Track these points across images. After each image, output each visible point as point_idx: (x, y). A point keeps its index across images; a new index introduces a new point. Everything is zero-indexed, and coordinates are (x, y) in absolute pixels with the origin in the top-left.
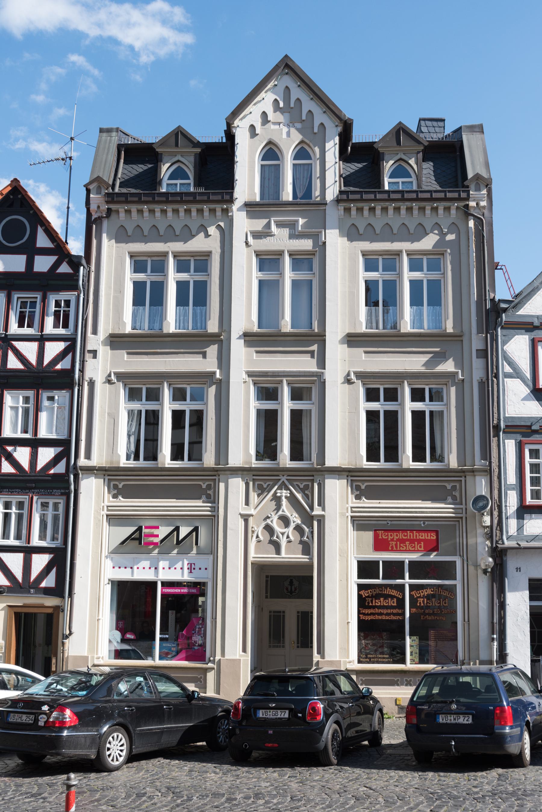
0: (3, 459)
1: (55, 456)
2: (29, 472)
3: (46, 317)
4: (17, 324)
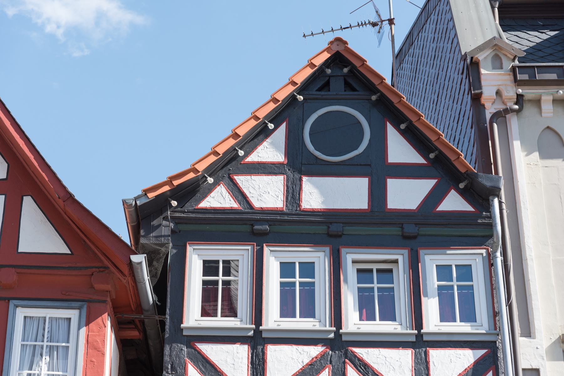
3: (423, 299)
4: (357, 314)
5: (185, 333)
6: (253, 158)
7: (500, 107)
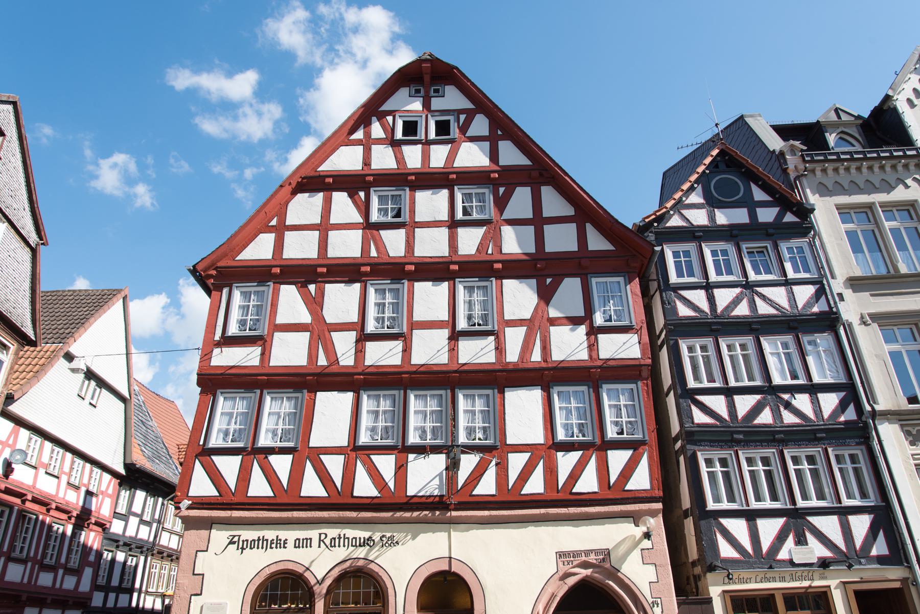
0: (782, 409)
1: (840, 402)
2: (816, 421)
5: (671, 286)
6: (688, 201)
7: (797, 174)
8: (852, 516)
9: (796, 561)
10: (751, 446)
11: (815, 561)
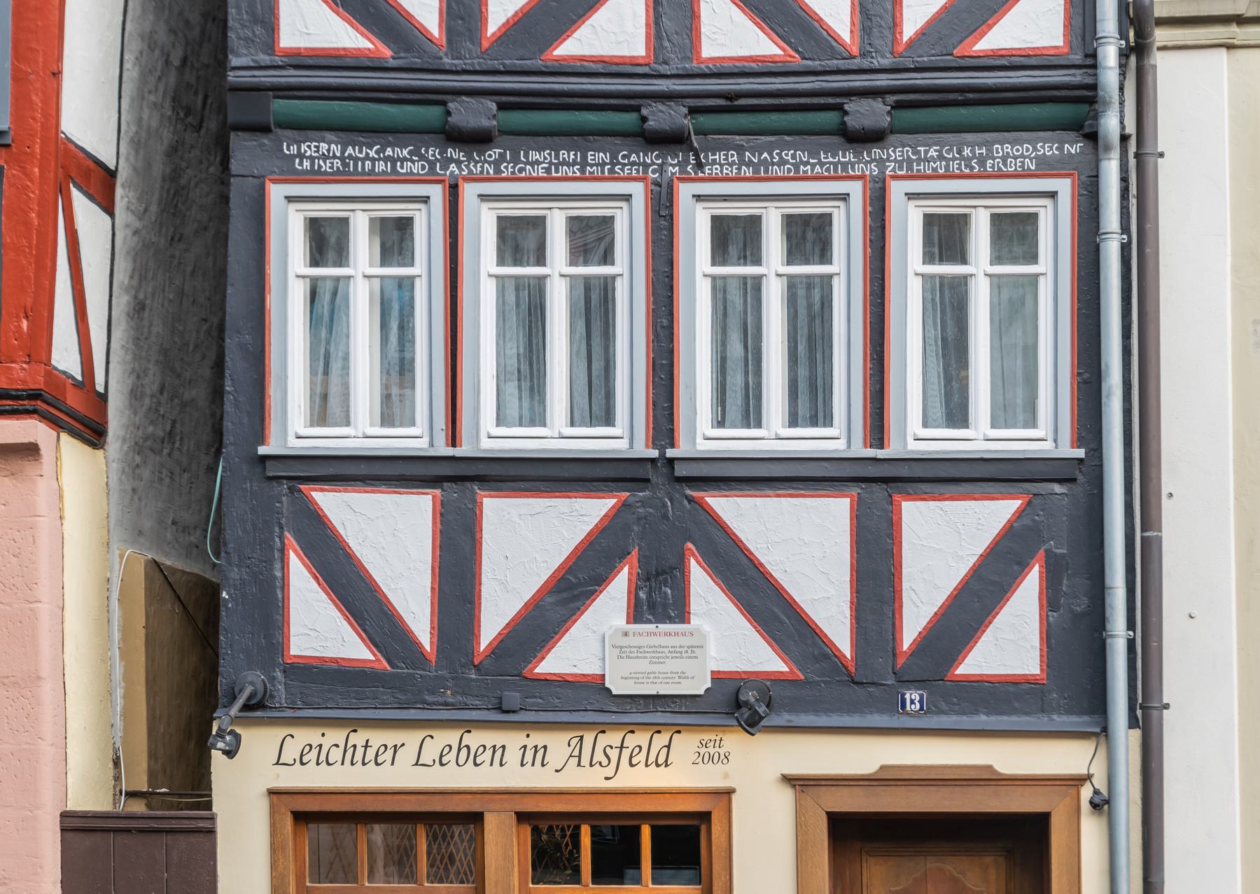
8: (920, 504)
9: (617, 686)
10: (532, 164)
11: (700, 686)
